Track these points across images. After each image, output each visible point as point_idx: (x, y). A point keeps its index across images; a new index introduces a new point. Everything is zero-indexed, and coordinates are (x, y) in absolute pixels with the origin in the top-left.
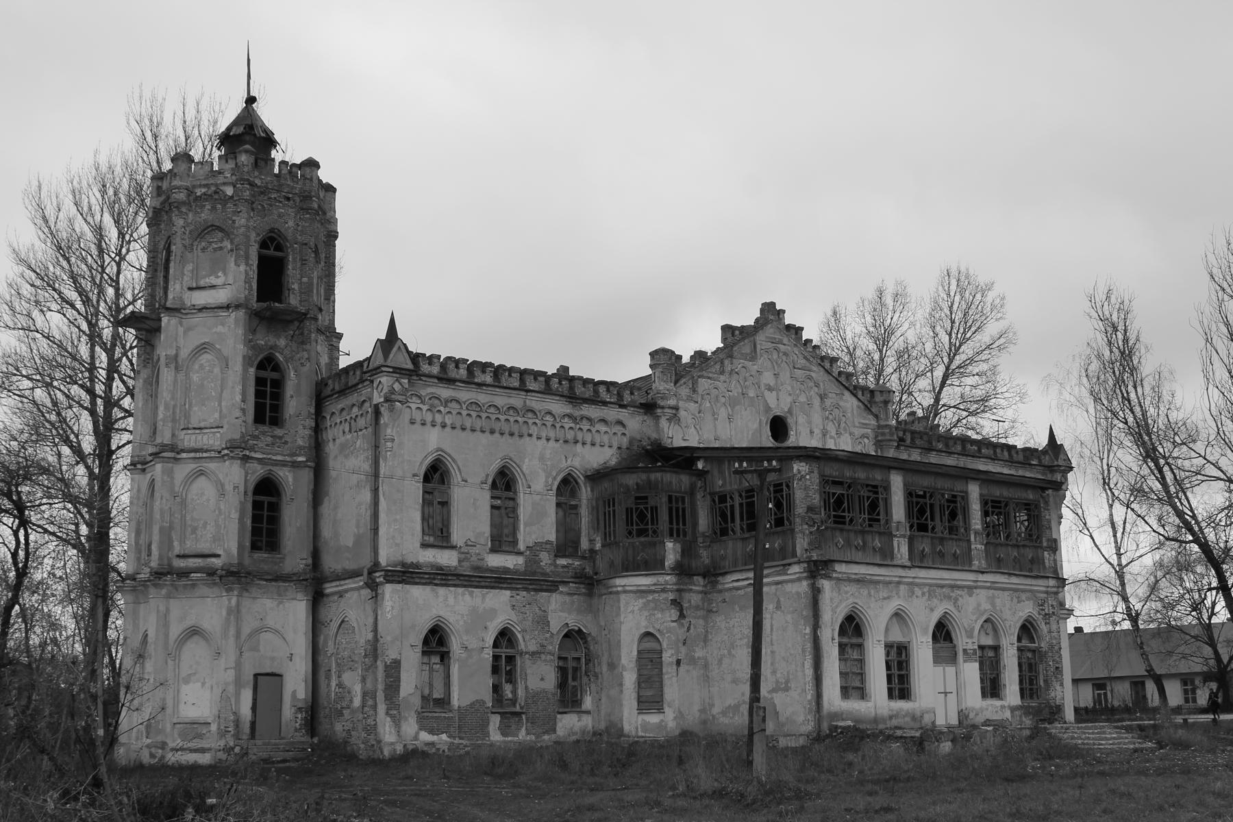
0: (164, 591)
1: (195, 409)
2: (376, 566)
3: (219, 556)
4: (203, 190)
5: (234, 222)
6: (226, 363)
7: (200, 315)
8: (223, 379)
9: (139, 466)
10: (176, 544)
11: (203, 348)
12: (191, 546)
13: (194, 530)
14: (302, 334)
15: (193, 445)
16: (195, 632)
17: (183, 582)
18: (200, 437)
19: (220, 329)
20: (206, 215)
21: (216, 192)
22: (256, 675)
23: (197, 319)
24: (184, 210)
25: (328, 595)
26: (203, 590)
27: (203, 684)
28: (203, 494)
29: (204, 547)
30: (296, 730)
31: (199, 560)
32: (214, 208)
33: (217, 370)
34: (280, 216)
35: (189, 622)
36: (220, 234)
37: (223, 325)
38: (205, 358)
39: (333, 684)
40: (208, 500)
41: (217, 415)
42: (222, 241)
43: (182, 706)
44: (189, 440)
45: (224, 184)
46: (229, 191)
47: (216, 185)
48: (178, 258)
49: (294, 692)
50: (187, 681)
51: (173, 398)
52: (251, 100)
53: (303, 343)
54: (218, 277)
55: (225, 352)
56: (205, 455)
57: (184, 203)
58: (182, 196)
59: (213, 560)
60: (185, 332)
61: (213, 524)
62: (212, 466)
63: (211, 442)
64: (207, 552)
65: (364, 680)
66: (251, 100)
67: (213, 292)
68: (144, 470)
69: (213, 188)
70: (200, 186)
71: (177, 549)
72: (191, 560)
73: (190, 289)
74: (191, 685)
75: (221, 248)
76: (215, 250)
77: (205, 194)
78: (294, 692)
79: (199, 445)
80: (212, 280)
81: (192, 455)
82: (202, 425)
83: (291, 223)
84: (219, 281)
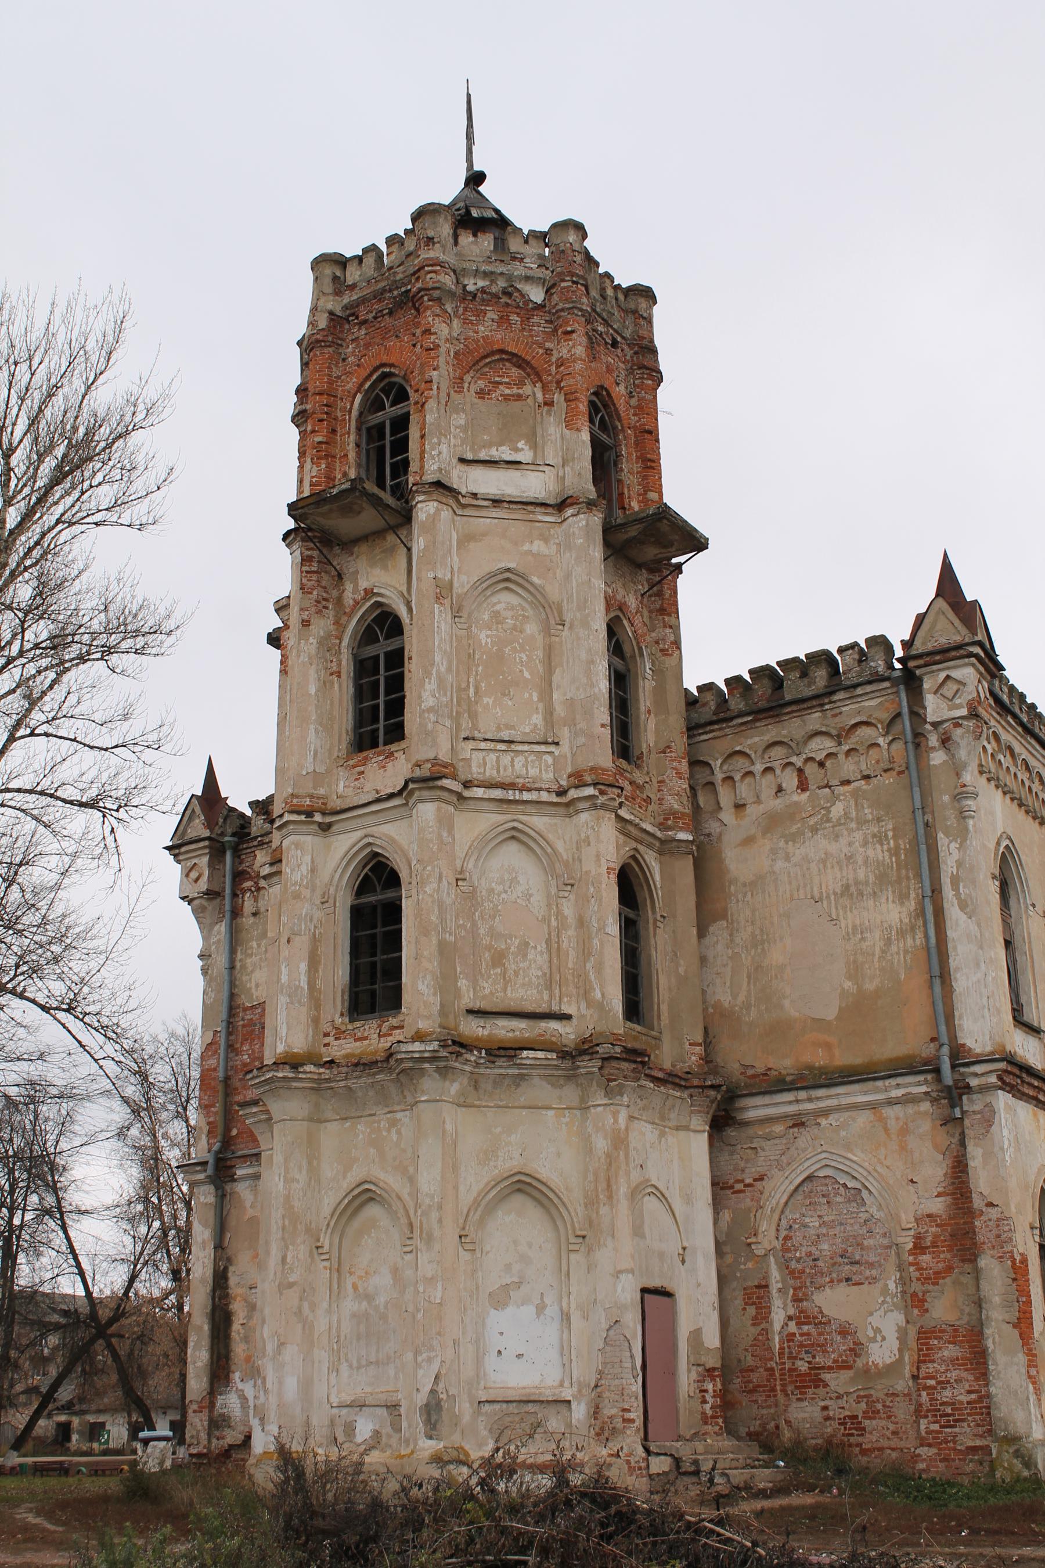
0: (454, 1088)
1: (487, 700)
2: (960, 1056)
3: (568, 1017)
4: (481, 283)
5: (548, 352)
6: (553, 618)
7: (495, 513)
8: (549, 651)
9: (318, 817)
10: (463, 983)
11: (507, 579)
12: (488, 991)
13: (499, 959)
14: (660, 594)
15: (490, 773)
16: (524, 1186)
17: (503, 1068)
18: (506, 759)
19: (538, 546)
20: (487, 328)
21: (506, 293)
22: (644, 1291)
23: (486, 522)
24: (449, 308)
25: (746, 1124)
26: (539, 1090)
27: (540, 1309)
28: (514, 881)
29: (527, 994)
30: (705, 1419)
31: (522, 1024)
32: (503, 320)
33: (531, 628)
34: (609, 370)
35: (508, 1161)
36: (515, 372)
37: (546, 540)
38: (504, 601)
39: (778, 1317)
40: (528, 896)
41: (537, 719)
42: (521, 384)
43: (491, 1361)
44: (481, 763)
45: (528, 279)
46: (537, 295)
47: (510, 278)
48: (443, 395)
49: (696, 1336)
50: (500, 1299)
51: (449, 669)
52: (476, 179)
53: (662, 611)
54: (517, 450)
55: (553, 592)
56: (526, 796)
57: (452, 294)
58: (448, 280)
59: (554, 1025)
60: (460, 544)
61: (542, 947)
62: (539, 822)
63: (533, 772)
64: (530, 1008)
65: (915, 1302)
66: (476, 179)
67: (513, 474)
68: (325, 828)
69: (502, 283)
70: (476, 273)
71: (468, 999)
72: (502, 1022)
73: (462, 460)
74: (510, 1309)
75: (519, 397)
76: (506, 398)
77: (483, 290)
78: (696, 1336)
79: (506, 776)
80: (505, 453)
81: (497, 793)
82: (505, 735)
83: (621, 389)
84: (525, 455)
